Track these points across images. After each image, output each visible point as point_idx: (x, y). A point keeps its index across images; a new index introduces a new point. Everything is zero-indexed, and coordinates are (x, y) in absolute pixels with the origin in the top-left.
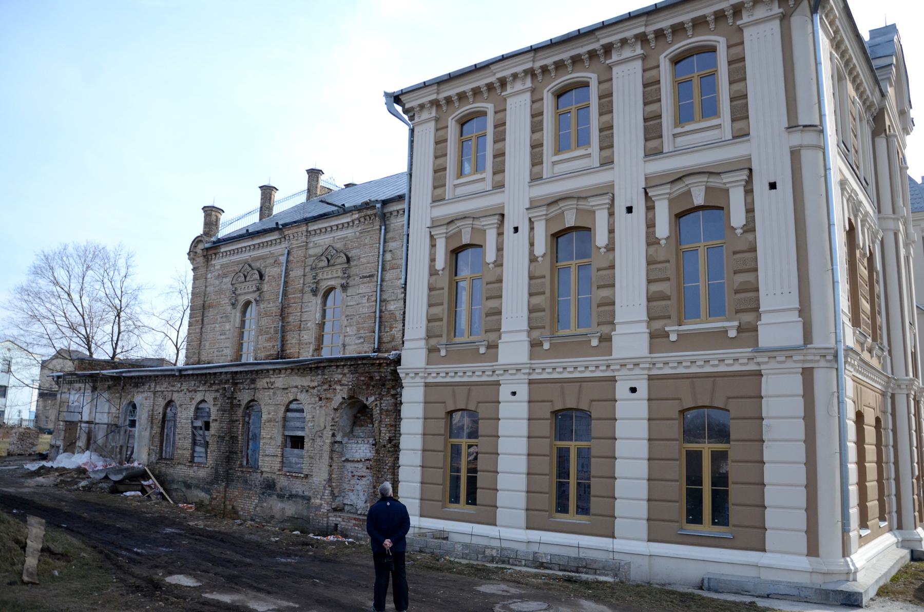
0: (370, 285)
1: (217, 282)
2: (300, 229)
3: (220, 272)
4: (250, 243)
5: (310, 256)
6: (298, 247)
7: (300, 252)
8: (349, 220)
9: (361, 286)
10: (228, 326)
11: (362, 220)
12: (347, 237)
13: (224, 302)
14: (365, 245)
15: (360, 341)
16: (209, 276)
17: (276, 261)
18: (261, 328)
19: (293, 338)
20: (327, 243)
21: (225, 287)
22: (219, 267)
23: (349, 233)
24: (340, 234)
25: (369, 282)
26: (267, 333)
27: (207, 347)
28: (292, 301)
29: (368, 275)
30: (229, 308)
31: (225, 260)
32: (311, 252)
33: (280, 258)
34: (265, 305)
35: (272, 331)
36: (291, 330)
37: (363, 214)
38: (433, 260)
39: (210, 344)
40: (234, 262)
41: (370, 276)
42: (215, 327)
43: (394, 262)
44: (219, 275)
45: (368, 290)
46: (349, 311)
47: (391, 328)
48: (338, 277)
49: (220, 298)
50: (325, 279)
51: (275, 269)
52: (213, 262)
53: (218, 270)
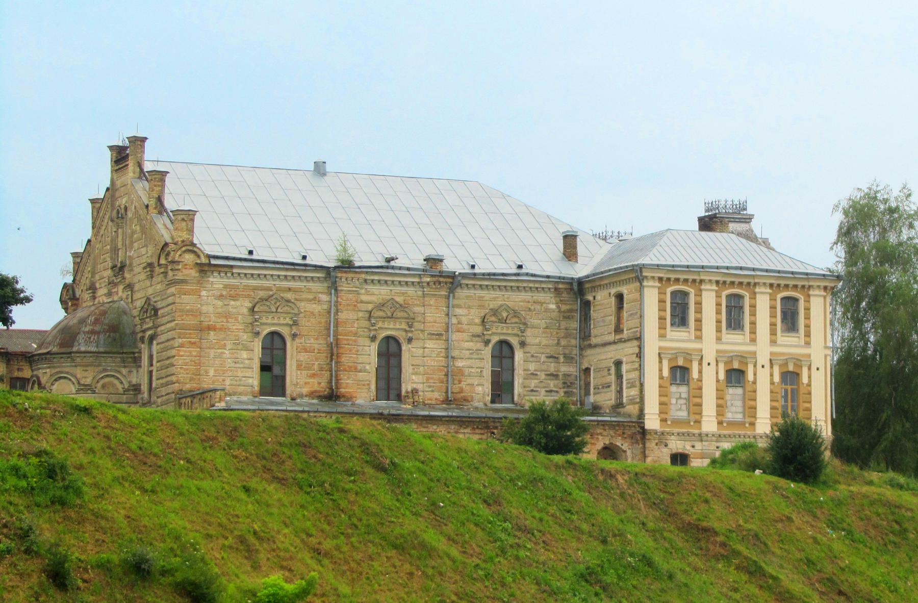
0: (438, 341)
1: (220, 303)
2: (358, 276)
3: (224, 293)
4: (283, 273)
5: (362, 302)
6: (349, 291)
7: (351, 295)
8: (416, 280)
9: (428, 341)
10: (244, 355)
11: (431, 284)
12: (406, 293)
13: (234, 327)
14: (431, 305)
15: (430, 389)
16: (204, 293)
17: (315, 298)
18: (300, 363)
19: (348, 378)
20: (382, 293)
21: (234, 310)
22: (221, 286)
23: (411, 290)
24: (399, 289)
25: (437, 339)
26: (308, 369)
27: (212, 373)
28: (346, 342)
29: (436, 332)
30: (245, 337)
31: (233, 281)
32: (364, 298)
33: (320, 295)
34: (303, 340)
35: (316, 367)
36: (345, 370)
37: (434, 279)
38: (661, 370)
39: (215, 371)
40: (248, 286)
41: (438, 335)
42: (222, 353)
43: (460, 326)
44: (222, 296)
45: (436, 346)
46: (416, 361)
47: (460, 382)
48: (402, 329)
49: (228, 322)
50: (386, 328)
51: (314, 306)
52: (211, 279)
53: (218, 289)
